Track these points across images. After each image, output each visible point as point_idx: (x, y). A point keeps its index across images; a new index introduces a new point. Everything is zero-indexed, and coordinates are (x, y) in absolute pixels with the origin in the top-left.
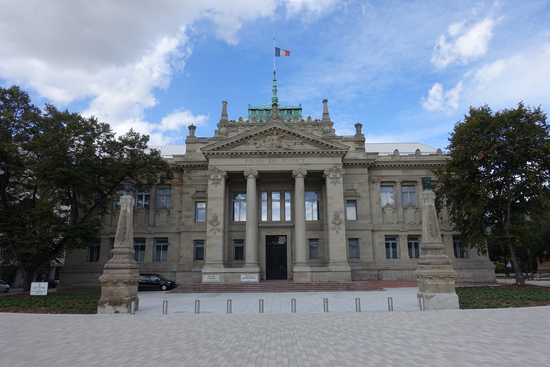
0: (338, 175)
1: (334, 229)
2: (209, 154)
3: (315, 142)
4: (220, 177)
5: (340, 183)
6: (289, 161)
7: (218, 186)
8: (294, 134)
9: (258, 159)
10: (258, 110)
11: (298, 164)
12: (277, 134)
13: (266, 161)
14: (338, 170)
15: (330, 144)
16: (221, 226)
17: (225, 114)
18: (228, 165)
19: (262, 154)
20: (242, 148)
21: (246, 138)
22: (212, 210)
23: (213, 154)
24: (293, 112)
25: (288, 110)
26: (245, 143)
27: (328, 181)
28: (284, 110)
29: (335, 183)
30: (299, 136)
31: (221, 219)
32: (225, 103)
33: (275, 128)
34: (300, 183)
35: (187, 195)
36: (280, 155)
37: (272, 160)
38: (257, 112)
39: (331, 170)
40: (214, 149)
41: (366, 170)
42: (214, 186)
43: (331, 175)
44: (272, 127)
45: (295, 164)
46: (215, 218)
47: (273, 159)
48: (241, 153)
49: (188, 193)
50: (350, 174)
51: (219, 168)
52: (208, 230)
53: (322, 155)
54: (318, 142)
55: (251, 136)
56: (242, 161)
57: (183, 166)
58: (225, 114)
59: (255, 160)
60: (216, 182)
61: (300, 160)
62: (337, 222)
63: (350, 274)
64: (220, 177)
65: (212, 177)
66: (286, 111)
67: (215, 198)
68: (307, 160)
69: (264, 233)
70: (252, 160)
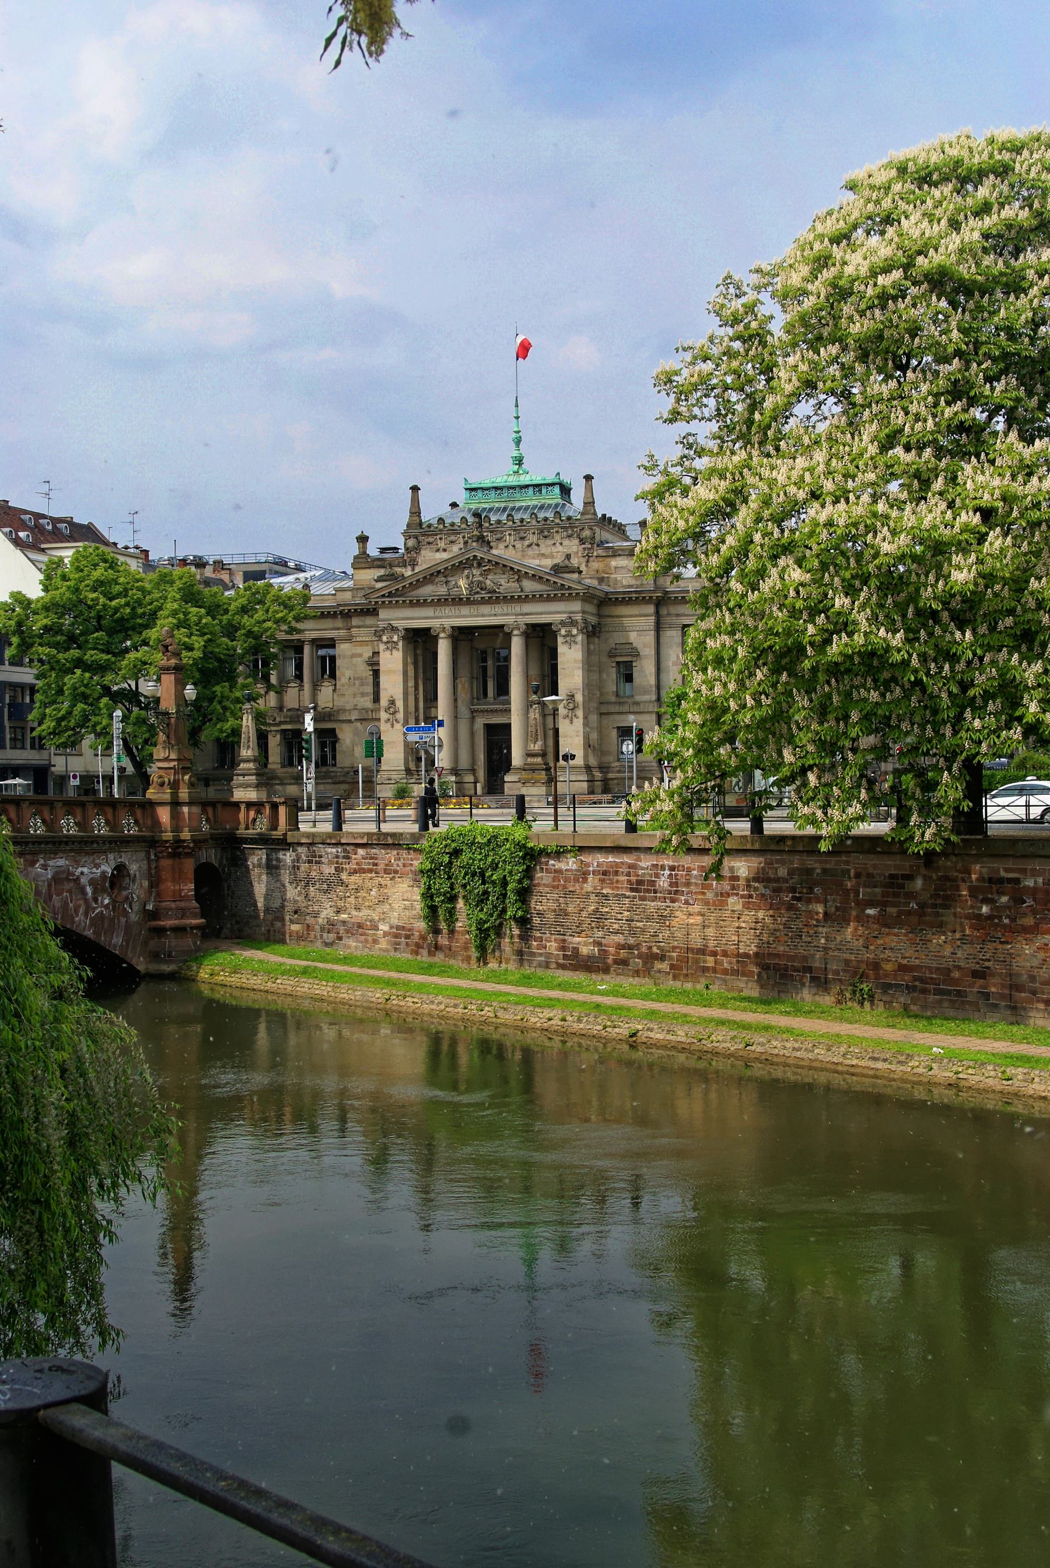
0: (575, 631)
1: (566, 717)
2: (376, 602)
3: (536, 577)
4: (395, 638)
5: (576, 643)
6: (498, 609)
7: (394, 651)
8: (504, 566)
9: (453, 608)
10: (482, 488)
11: (512, 615)
12: (479, 565)
13: (465, 610)
14: (573, 623)
15: (560, 582)
16: (400, 716)
17: (415, 511)
18: (408, 619)
19: (458, 601)
20: (427, 591)
21: (432, 575)
22: (386, 689)
23: (383, 602)
24: (544, 491)
25: (535, 486)
26: (432, 582)
27: (560, 640)
28: (527, 486)
29: (569, 644)
30: (512, 568)
31: (400, 704)
32: (415, 489)
33: (475, 556)
34: (517, 645)
35: (359, 659)
36: (483, 602)
37: (473, 610)
38: (480, 493)
39: (563, 623)
40: (383, 596)
41: (651, 609)
42: (389, 652)
43: (563, 632)
44: (470, 555)
45: (507, 615)
46: (392, 702)
47: (475, 607)
48: (425, 600)
49: (360, 655)
50: (622, 616)
51: (395, 623)
52: (382, 721)
53: (549, 599)
54: (540, 578)
55: (439, 572)
56: (429, 612)
57: (349, 610)
58: (415, 511)
59: (447, 609)
60: (391, 646)
61: (517, 608)
62: (571, 706)
63: (585, 785)
64: (395, 638)
65: (384, 638)
66: (531, 489)
67: (390, 672)
68: (527, 608)
69: (480, 722)
70: (443, 608)
